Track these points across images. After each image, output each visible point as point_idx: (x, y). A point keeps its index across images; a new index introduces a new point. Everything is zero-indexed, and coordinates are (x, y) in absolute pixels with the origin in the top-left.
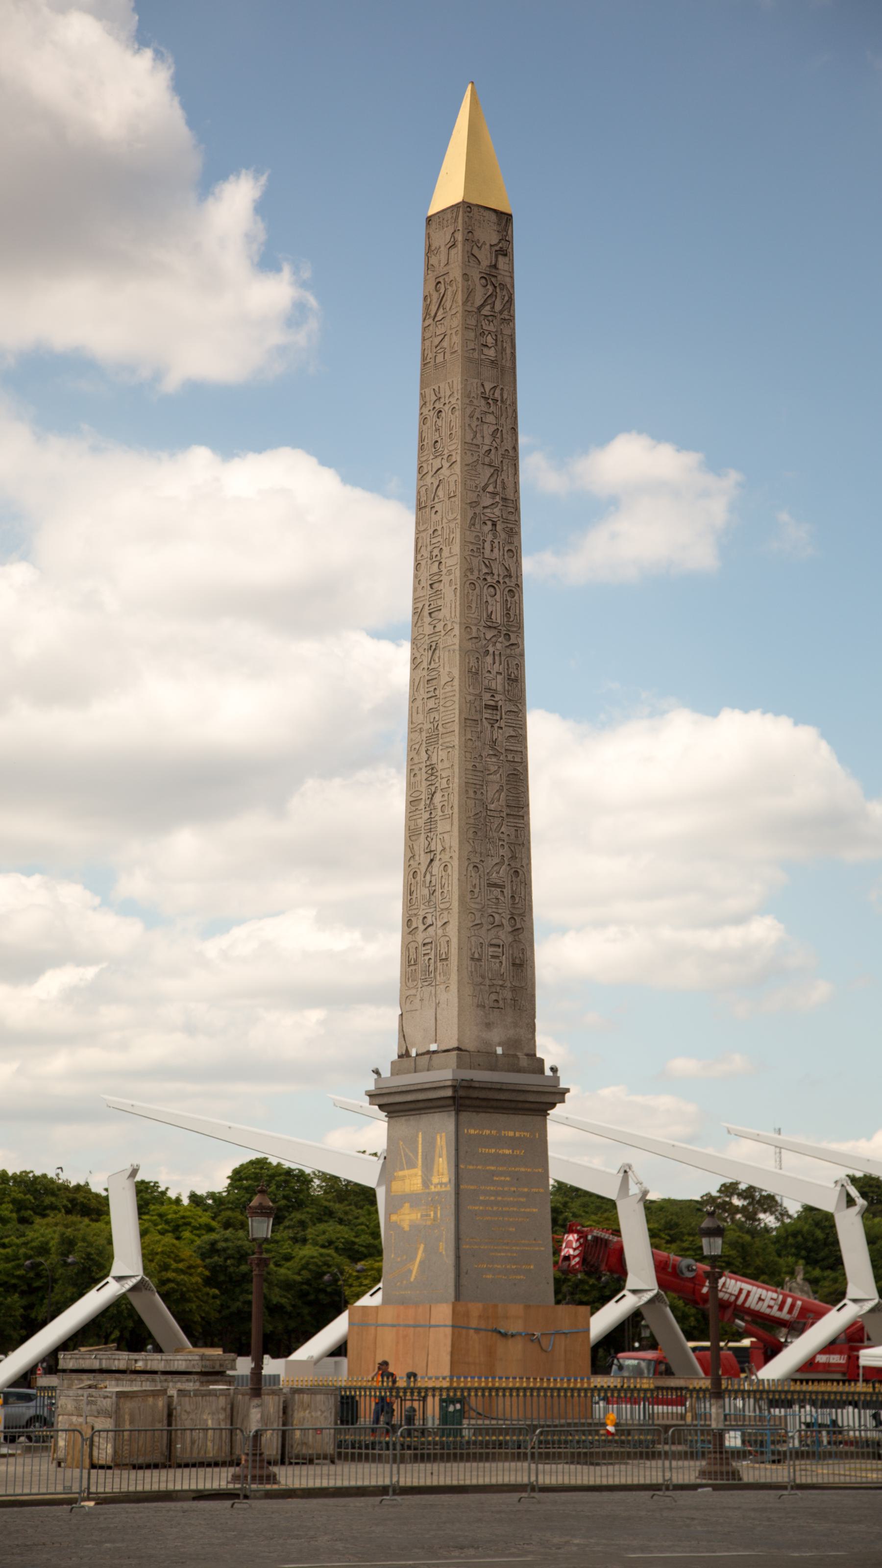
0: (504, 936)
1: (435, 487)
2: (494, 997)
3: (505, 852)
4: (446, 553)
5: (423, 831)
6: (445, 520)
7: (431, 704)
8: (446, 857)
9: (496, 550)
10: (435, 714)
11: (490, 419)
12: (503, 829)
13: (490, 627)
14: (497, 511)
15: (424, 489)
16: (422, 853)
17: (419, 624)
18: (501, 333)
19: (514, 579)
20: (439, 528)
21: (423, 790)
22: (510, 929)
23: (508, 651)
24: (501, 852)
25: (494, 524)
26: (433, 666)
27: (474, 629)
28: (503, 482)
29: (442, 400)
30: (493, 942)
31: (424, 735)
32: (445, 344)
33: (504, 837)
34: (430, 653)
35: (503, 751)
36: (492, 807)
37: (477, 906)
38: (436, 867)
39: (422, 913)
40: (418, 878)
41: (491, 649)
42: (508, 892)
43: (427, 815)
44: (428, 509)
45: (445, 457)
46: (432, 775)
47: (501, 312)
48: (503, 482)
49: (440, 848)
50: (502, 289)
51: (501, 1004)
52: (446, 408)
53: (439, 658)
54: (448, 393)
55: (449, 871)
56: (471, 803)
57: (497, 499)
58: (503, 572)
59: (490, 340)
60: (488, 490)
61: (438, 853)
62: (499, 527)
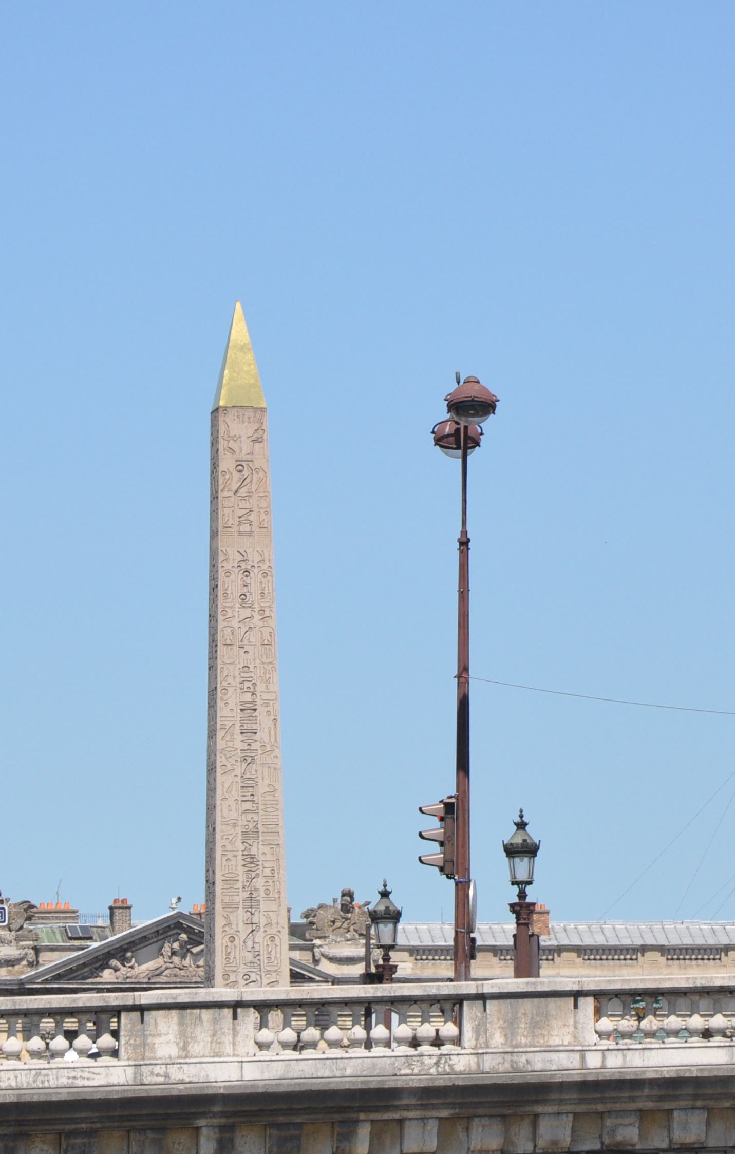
1: (244, 630)
4: (261, 687)
5: (241, 906)
6: (258, 662)
7: (248, 806)
8: (273, 931)
10: (254, 815)
15: (229, 630)
16: (241, 924)
17: (228, 738)
20: (251, 666)
21: (241, 874)
26: (248, 775)
29: (250, 563)
31: (239, 830)
32: (252, 517)
34: (244, 765)
38: (259, 937)
39: (243, 969)
40: (236, 942)
43: (247, 894)
44: (236, 648)
45: (257, 610)
46: (251, 863)
49: (263, 922)
52: (256, 570)
53: (256, 771)
54: (257, 558)
55: (277, 941)
61: (262, 925)
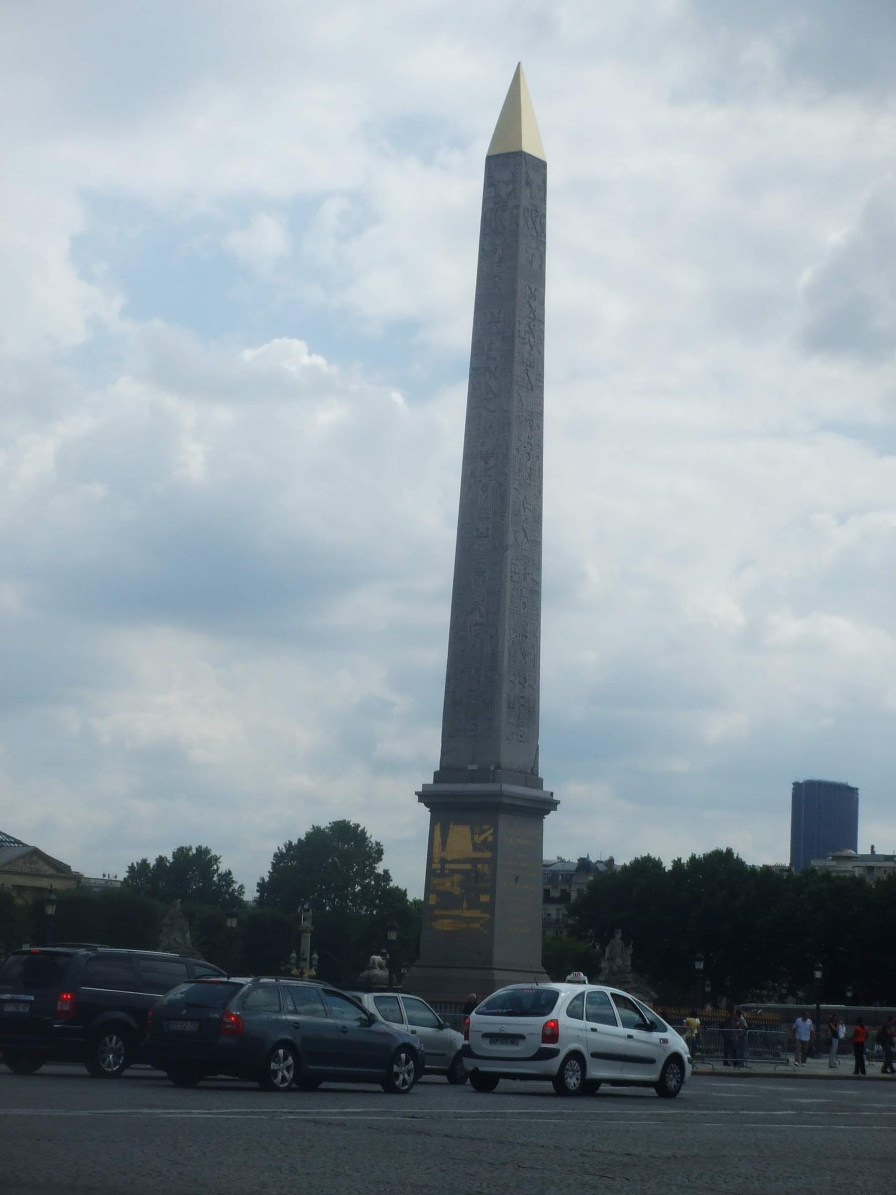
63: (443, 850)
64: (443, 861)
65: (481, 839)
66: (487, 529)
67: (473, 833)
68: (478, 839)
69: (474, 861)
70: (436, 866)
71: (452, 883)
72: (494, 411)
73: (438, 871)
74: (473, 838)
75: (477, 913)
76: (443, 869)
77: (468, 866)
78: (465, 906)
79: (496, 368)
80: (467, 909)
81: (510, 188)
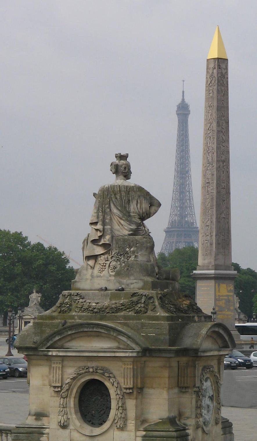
0: (209, 238)
2: (206, 253)
3: (209, 217)
9: (210, 144)
11: (210, 111)
12: (209, 212)
13: (208, 163)
14: (211, 134)
18: (214, 89)
19: (214, 150)
22: (210, 236)
23: (212, 168)
24: (209, 218)
25: (210, 137)
27: (205, 165)
28: (213, 126)
30: (207, 239)
33: (210, 214)
35: (210, 193)
36: (207, 207)
37: (203, 232)
41: (208, 169)
42: (210, 227)
47: (214, 84)
48: (213, 126)
50: (214, 78)
51: (207, 254)
56: (203, 207)
57: (211, 131)
58: (212, 149)
59: (211, 91)
60: (209, 129)
62: (211, 138)
63: (219, 292)
64: (219, 296)
65: (230, 288)
66: (225, 186)
67: (227, 287)
68: (229, 289)
69: (227, 296)
70: (217, 297)
71: (222, 303)
72: (224, 147)
73: (218, 299)
74: (227, 288)
75: (229, 313)
76: (219, 298)
77: (226, 298)
78: (226, 310)
79: (224, 132)
80: (227, 311)
81: (225, 71)
